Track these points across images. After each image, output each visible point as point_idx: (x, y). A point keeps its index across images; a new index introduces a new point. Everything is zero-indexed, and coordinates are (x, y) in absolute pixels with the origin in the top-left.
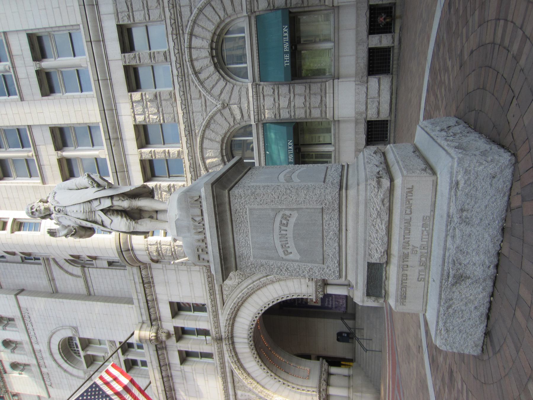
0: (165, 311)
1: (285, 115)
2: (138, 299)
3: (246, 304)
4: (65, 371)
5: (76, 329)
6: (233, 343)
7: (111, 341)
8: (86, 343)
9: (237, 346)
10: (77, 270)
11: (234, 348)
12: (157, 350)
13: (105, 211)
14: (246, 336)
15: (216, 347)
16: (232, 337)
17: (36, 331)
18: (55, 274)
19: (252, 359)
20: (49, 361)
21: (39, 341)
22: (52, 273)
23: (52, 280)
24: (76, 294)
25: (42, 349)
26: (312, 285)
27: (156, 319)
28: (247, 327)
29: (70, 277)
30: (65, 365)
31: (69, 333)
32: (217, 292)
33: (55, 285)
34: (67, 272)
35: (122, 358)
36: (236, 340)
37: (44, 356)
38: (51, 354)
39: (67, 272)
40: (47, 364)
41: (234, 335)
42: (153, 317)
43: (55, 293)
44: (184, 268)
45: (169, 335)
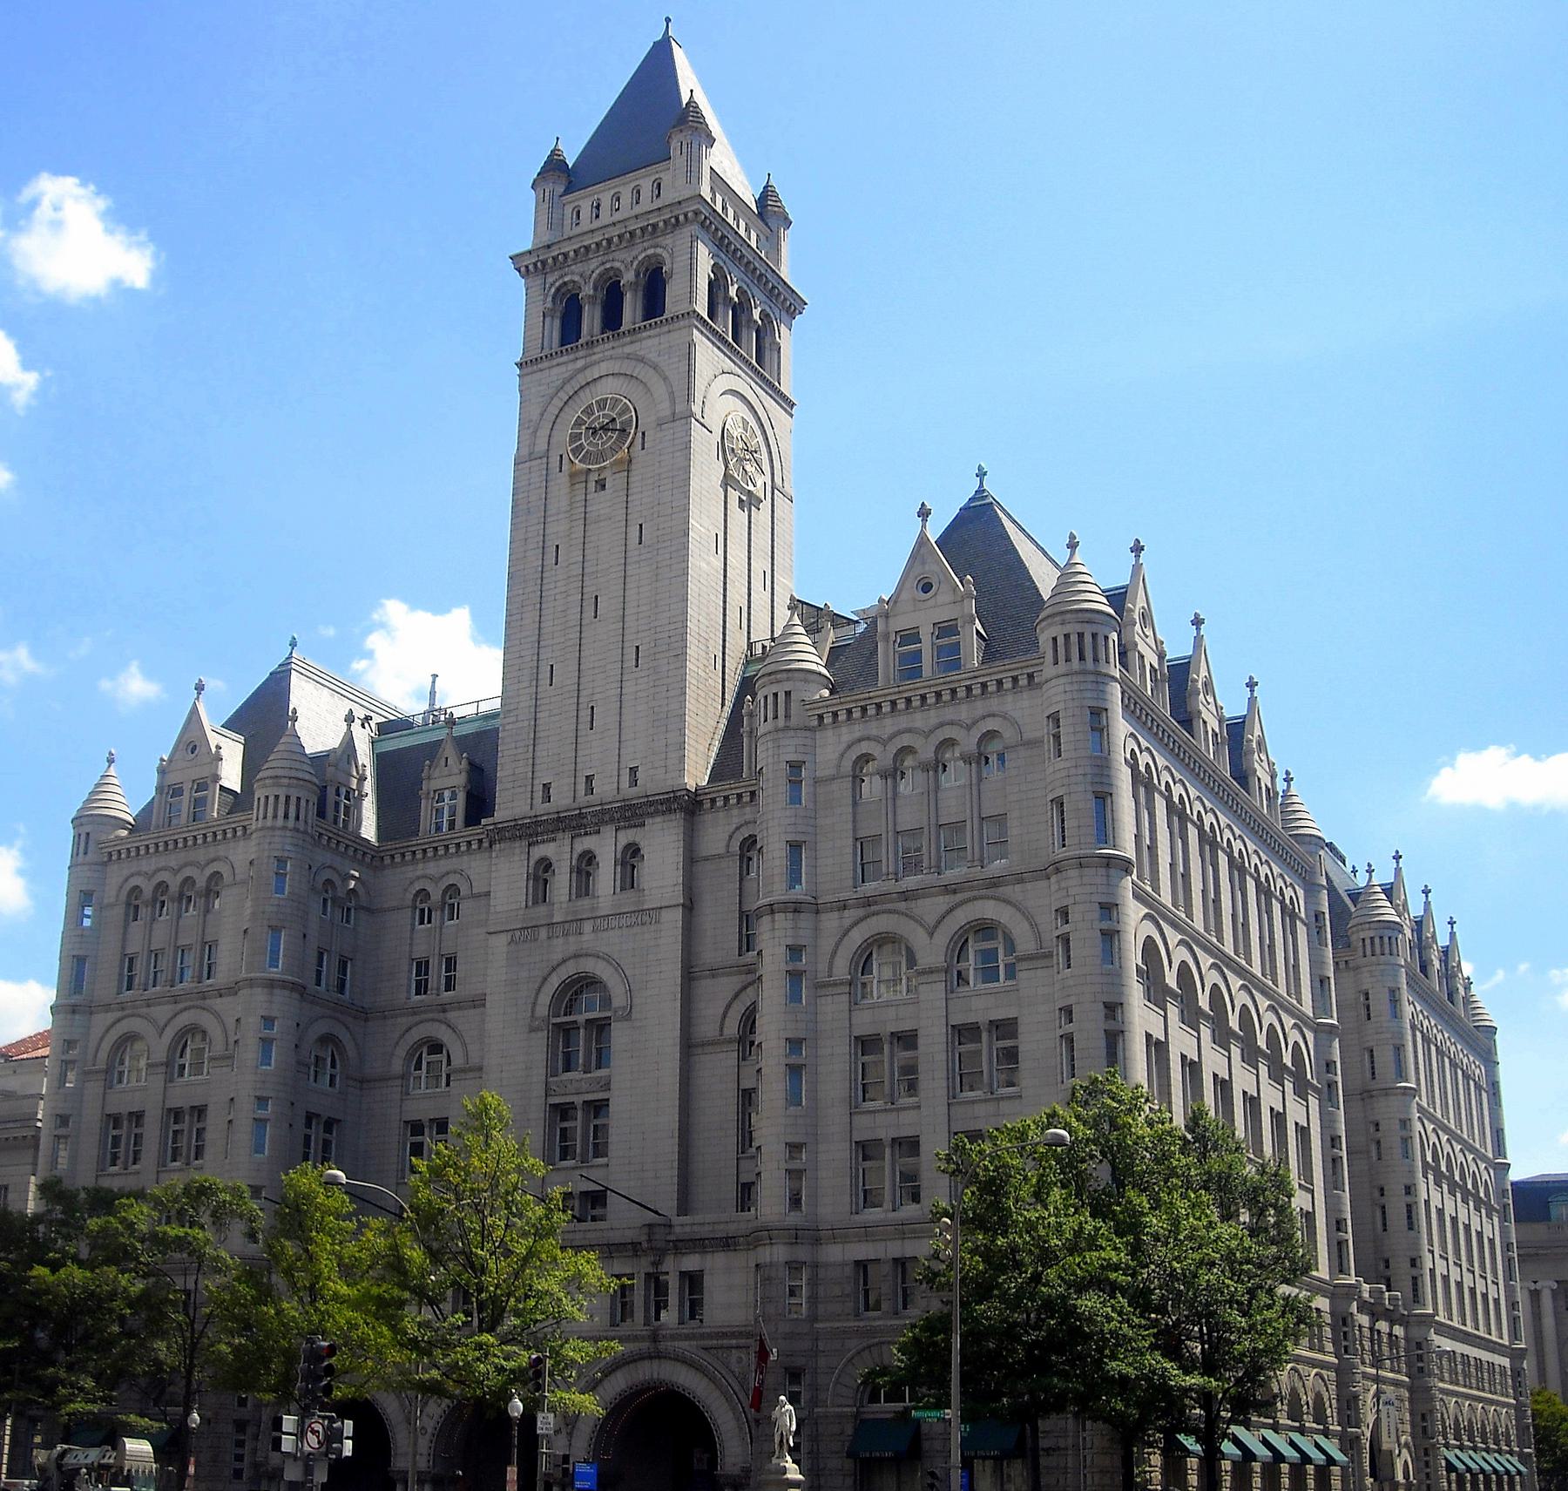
0: (691, 1263)
1: (926, 1445)
2: (703, 1224)
3: (706, 1380)
4: (545, 979)
5: (628, 1017)
6: (651, 1358)
7: (609, 1083)
8: (600, 1028)
9: (647, 1363)
10: (732, 1028)
11: (642, 1359)
12: (632, 1243)
13: (782, 1433)
14: (662, 1377)
15: (644, 1333)
16: (659, 1357)
17: (617, 932)
18: (724, 980)
19: (630, 1383)
20: (560, 947)
21: (600, 934)
22: (723, 975)
23: (714, 972)
24: (689, 1018)
25: (585, 938)
26: (736, 1471)
27: (676, 1248)
28: (674, 1379)
29: (721, 1011)
30: (555, 981)
31: (618, 1000)
32: (720, 1342)
33: (706, 977)
34: (728, 1006)
35: (578, 1100)
36: (656, 1362)
37: (571, 939)
38: (576, 956)
39: (728, 1006)
40: (555, 941)
41: (662, 1360)
42: (680, 1244)
43: (689, 975)
44: (751, 1298)
45: (656, 1264)
